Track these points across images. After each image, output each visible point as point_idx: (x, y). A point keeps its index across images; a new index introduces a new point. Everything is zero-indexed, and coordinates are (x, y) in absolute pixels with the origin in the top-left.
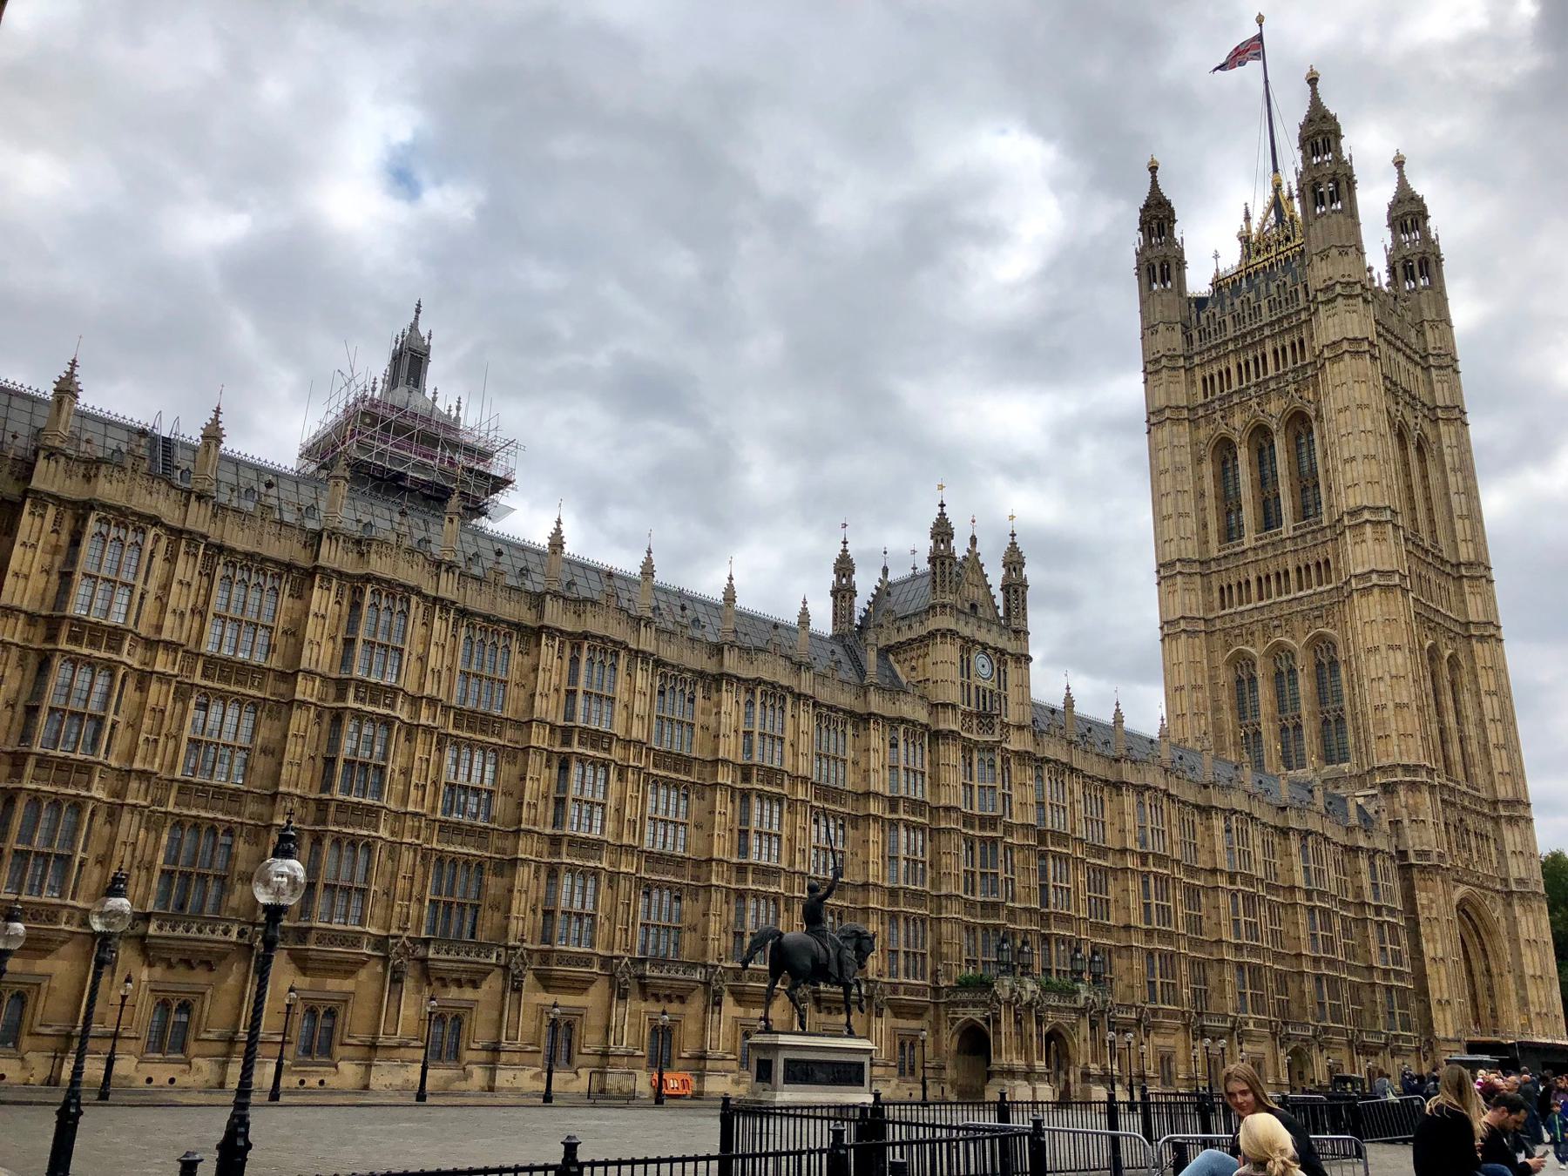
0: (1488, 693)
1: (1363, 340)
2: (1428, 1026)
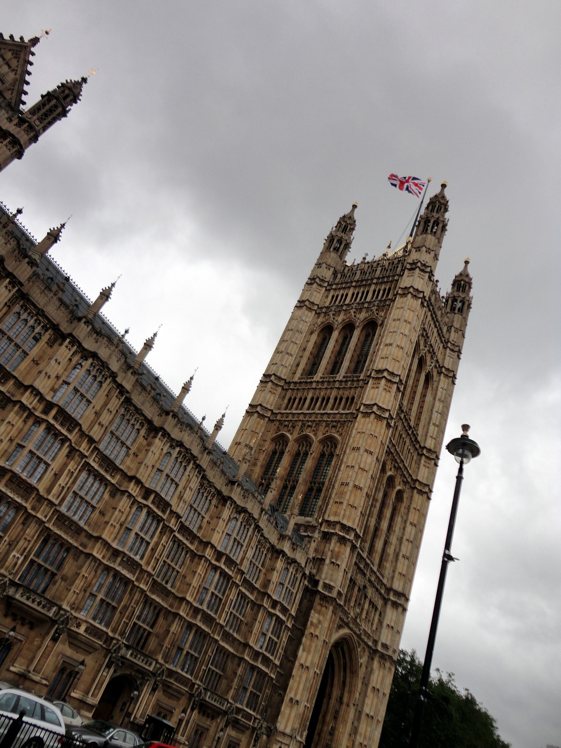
0: (411, 524)
1: (421, 292)
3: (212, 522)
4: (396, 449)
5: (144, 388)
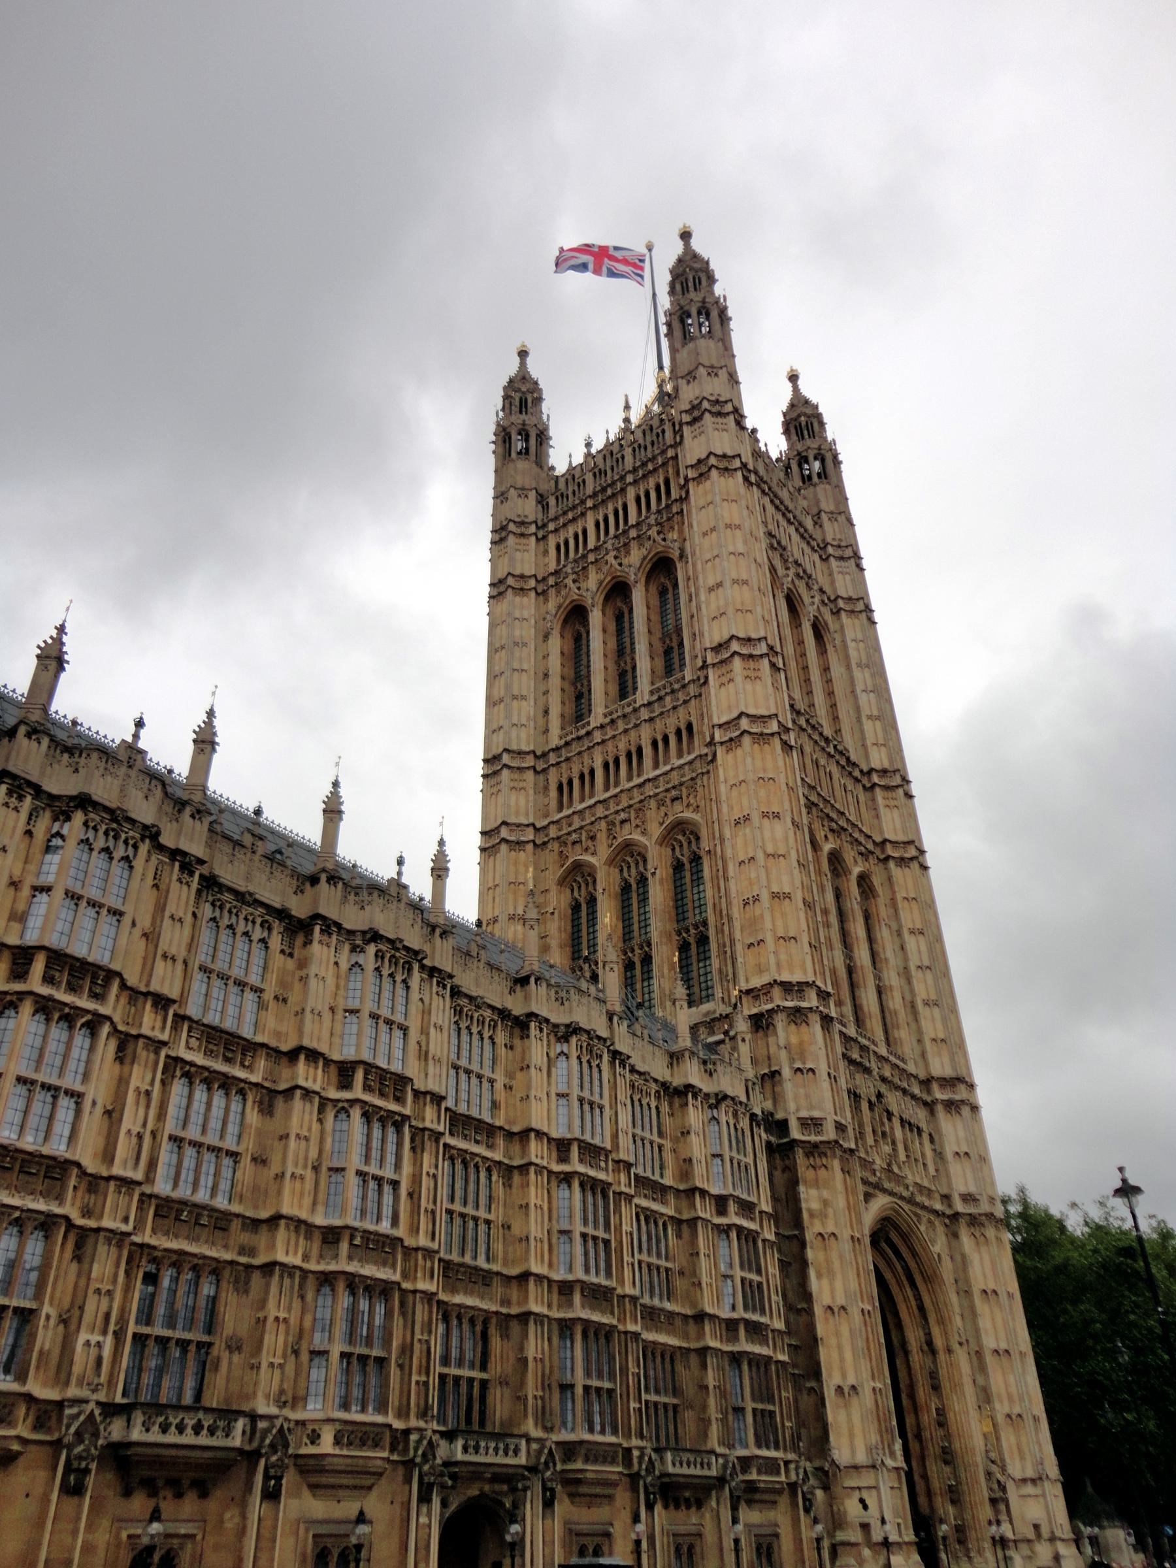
0: (912, 932)
2: (821, 1442)
3: (513, 1083)
4: (819, 794)
5: (237, 844)
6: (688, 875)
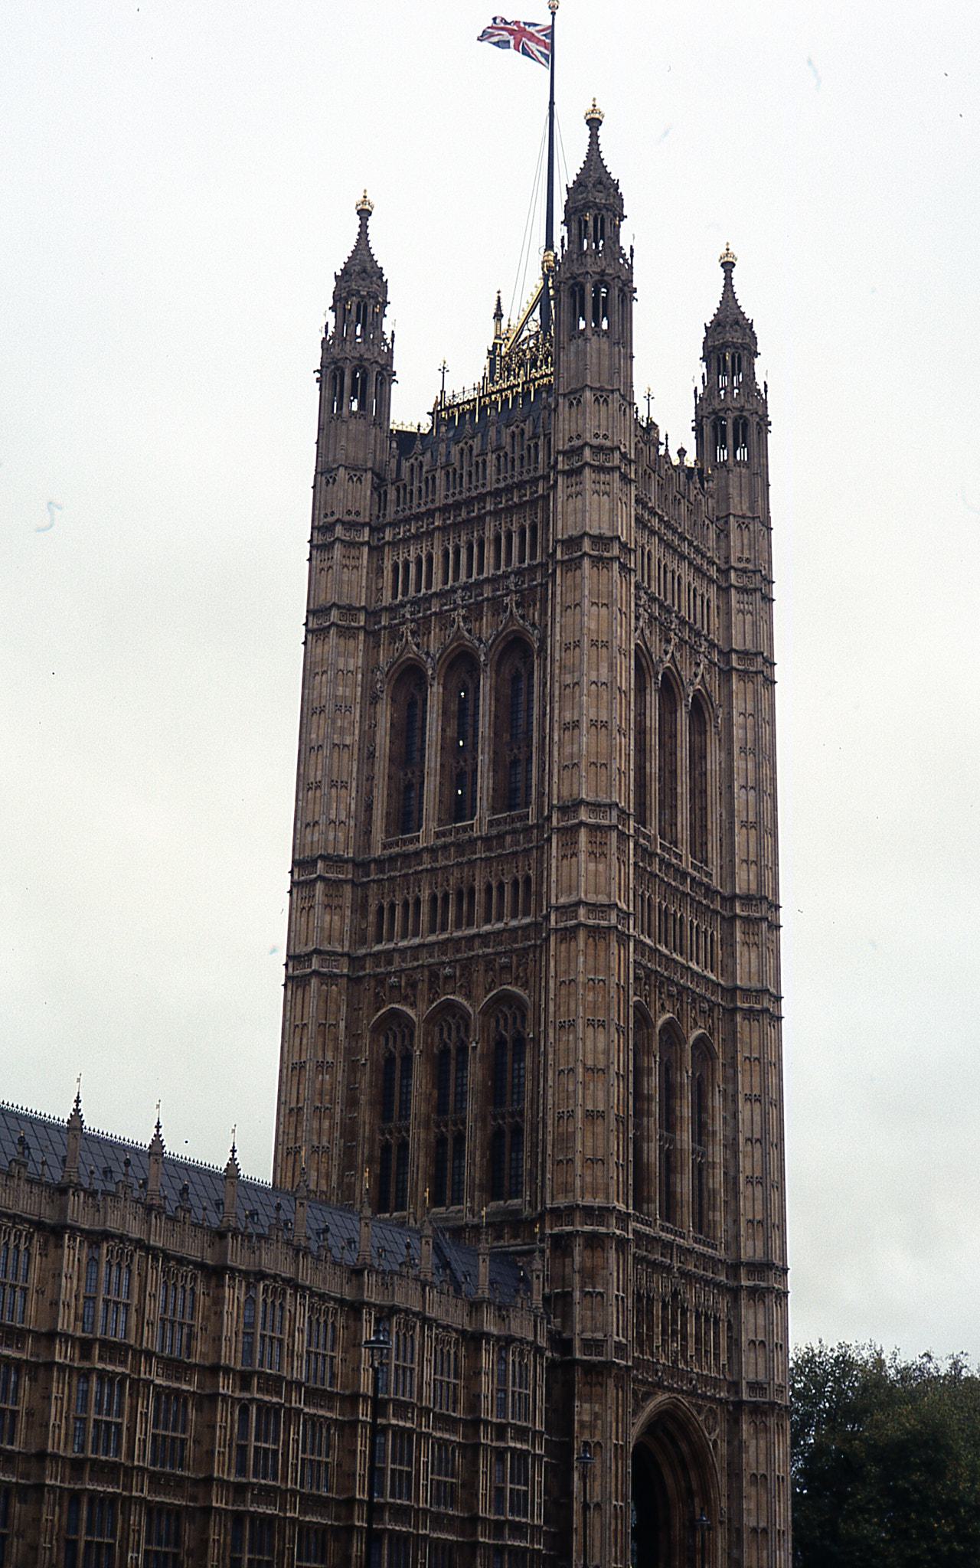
0: (748, 1098)
6: (509, 1054)
